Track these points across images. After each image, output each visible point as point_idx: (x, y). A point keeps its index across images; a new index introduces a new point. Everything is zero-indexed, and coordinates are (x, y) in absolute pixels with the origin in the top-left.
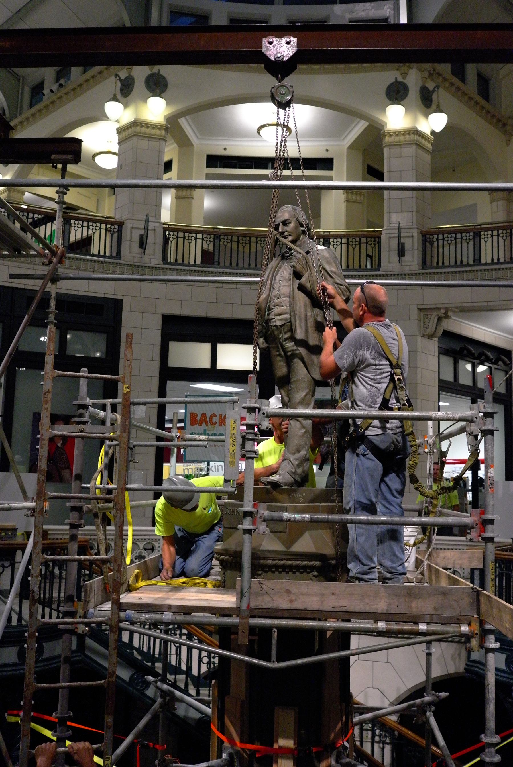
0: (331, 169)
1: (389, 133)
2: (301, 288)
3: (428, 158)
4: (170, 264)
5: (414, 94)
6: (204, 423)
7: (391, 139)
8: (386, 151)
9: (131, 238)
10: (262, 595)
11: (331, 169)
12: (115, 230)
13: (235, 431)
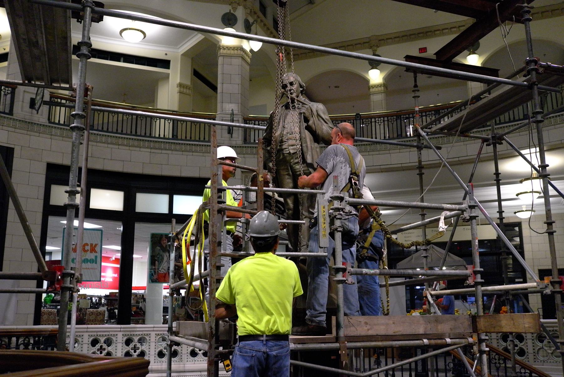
0: (169, 68)
1: (223, 47)
2: (308, 128)
3: (248, 67)
4: (54, 123)
5: (240, 23)
7: (225, 51)
8: (220, 60)
9: (23, 99)
10: (350, 327)
11: (169, 68)
12: (9, 92)
13: (325, 213)
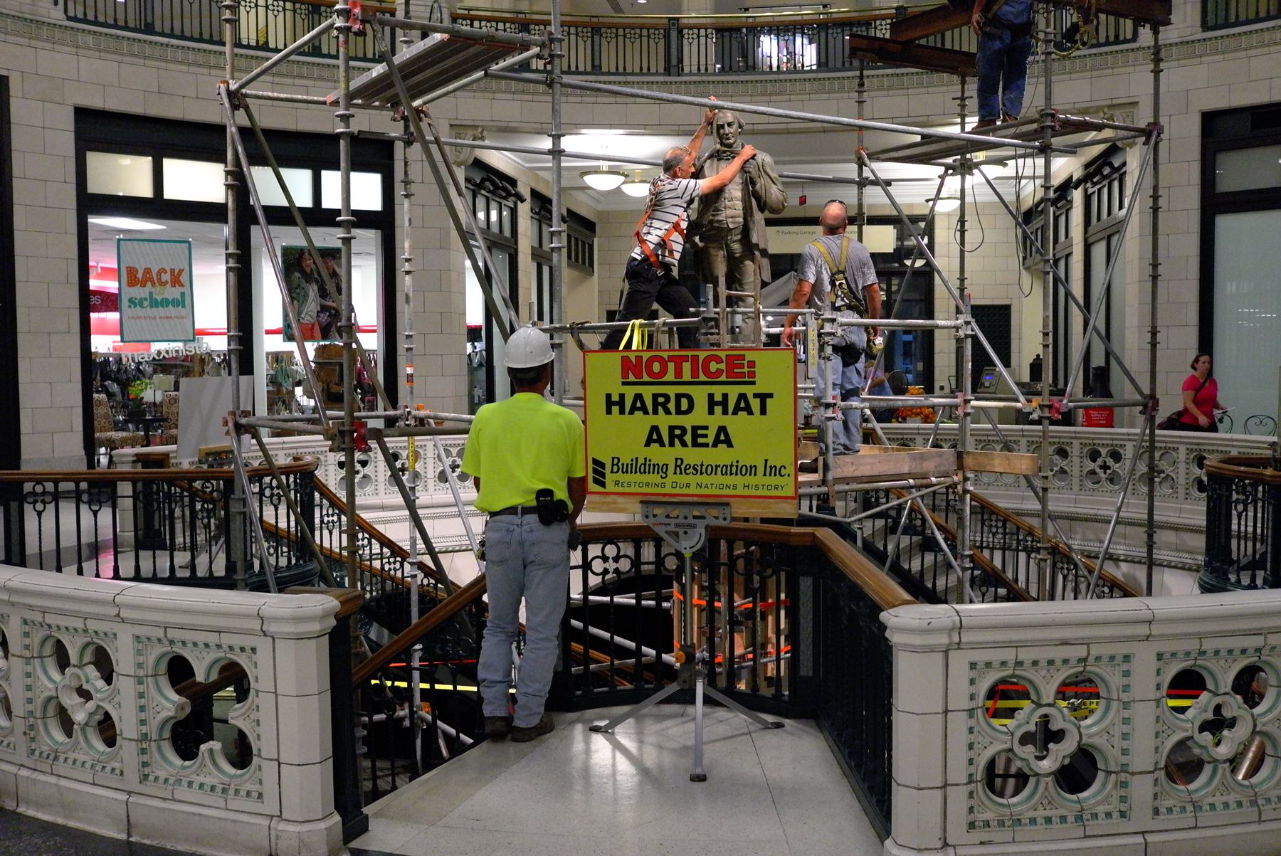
6: (149, 284)
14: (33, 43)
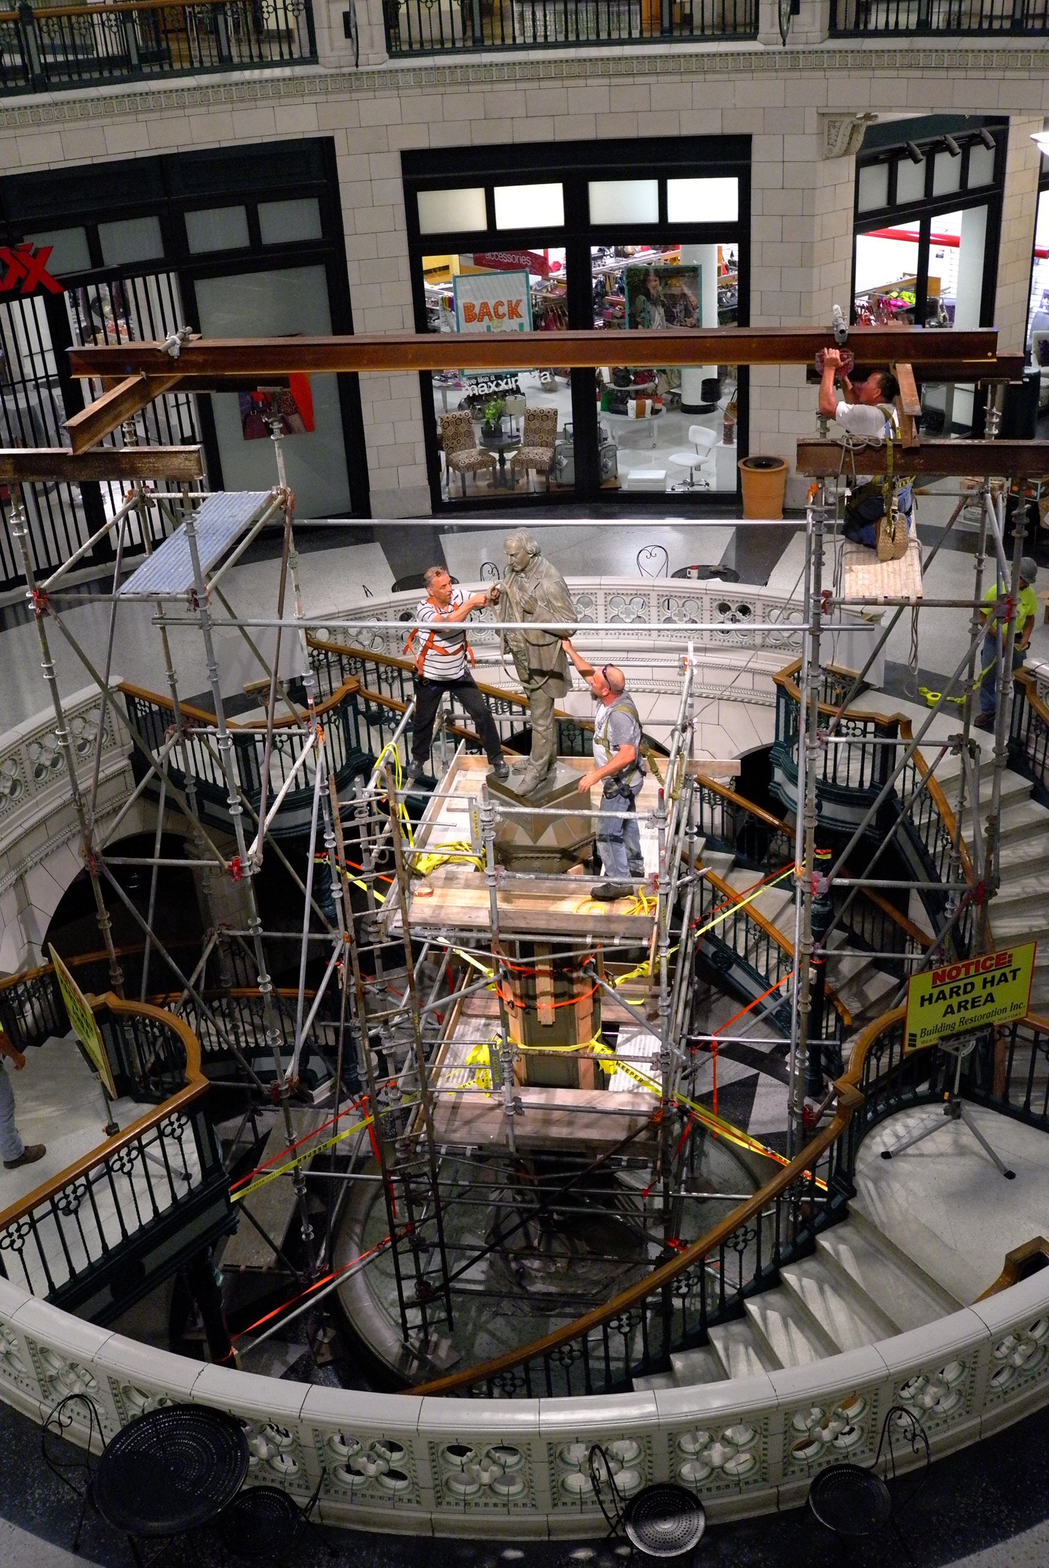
9: (329, 22)
14: (355, 96)
